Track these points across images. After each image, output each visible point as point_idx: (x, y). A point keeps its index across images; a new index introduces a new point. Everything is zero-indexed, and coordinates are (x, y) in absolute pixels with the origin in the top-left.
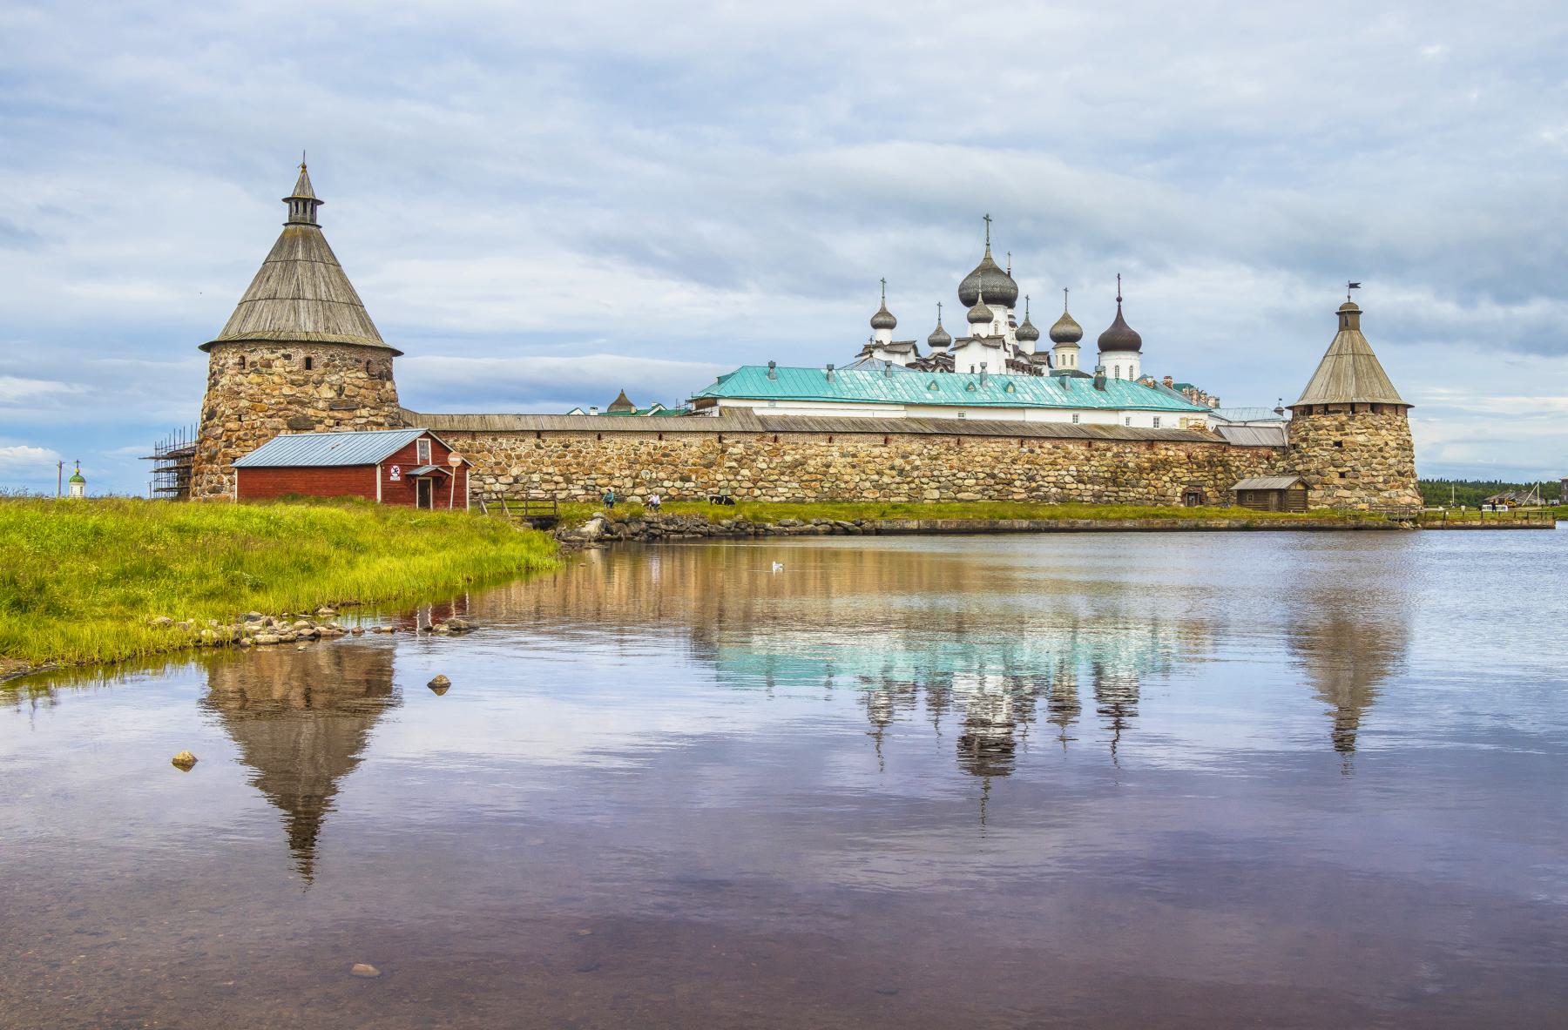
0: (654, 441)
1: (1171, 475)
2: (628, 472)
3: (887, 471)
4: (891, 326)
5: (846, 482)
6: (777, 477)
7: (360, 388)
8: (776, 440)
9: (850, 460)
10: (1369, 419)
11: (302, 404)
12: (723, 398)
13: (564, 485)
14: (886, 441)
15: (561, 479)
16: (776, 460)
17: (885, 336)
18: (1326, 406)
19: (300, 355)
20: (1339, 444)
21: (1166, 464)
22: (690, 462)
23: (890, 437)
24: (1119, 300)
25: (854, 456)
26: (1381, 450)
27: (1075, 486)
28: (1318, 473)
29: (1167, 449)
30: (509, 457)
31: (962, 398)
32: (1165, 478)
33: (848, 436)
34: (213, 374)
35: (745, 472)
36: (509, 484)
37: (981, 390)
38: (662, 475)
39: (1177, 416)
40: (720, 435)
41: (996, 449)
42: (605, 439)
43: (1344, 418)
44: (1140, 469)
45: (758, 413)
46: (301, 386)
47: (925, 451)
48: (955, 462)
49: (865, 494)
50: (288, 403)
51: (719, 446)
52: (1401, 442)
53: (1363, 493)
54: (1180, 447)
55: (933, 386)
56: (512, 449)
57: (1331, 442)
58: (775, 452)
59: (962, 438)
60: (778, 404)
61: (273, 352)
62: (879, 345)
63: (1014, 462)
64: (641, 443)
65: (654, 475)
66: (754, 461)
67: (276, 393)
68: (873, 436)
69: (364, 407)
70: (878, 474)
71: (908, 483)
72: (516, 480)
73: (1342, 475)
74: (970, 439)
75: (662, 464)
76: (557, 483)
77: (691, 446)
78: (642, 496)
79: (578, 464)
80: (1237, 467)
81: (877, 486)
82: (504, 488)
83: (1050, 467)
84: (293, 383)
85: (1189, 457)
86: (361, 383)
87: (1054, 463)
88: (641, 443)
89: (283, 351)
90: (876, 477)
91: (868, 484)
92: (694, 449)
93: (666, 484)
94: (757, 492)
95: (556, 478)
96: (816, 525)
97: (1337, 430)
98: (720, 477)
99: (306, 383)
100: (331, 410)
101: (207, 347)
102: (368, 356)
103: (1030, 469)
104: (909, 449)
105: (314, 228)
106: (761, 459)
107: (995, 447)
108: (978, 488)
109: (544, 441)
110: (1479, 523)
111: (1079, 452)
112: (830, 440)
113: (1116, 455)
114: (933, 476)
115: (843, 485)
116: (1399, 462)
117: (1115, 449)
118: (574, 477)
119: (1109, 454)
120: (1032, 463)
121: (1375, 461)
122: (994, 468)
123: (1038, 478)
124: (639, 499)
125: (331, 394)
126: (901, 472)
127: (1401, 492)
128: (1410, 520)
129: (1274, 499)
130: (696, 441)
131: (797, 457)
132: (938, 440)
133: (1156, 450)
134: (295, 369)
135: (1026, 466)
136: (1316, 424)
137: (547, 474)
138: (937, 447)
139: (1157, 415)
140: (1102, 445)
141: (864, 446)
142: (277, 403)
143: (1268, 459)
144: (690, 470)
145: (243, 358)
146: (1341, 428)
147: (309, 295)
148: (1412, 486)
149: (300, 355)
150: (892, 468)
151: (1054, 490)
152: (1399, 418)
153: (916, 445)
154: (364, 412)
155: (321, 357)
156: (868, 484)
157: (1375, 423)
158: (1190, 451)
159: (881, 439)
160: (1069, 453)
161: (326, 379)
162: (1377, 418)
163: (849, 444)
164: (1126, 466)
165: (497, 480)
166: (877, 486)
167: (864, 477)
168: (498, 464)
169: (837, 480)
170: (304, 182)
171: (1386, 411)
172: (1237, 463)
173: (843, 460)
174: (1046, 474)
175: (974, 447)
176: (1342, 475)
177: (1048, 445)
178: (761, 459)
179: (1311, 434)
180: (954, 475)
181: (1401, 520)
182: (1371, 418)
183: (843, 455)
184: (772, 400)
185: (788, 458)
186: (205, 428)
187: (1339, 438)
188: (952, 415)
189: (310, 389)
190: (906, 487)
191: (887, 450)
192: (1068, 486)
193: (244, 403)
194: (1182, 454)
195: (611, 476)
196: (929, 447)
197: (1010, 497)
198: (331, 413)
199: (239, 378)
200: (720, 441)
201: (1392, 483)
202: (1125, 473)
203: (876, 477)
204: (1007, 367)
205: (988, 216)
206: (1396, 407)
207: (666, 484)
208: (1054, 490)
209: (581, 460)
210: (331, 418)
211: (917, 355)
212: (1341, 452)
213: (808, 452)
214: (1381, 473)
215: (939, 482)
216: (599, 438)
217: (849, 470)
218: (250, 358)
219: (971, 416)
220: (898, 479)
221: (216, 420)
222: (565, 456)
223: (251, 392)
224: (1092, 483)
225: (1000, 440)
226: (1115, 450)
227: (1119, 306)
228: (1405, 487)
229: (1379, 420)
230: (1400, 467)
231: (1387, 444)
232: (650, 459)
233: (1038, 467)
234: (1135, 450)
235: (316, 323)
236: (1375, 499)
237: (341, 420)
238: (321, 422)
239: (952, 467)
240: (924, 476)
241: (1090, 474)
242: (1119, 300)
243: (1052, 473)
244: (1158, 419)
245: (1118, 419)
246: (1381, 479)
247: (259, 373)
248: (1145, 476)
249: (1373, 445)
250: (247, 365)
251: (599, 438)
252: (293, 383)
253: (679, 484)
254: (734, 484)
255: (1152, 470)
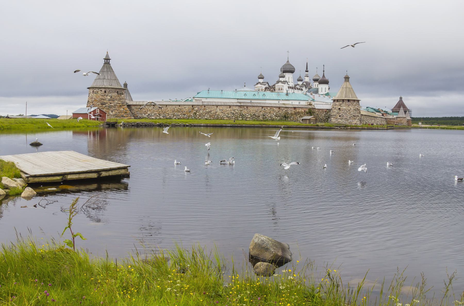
0: (178, 107)
1: (299, 115)
2: (172, 113)
3: (230, 114)
4: (263, 78)
5: (220, 116)
6: (205, 115)
7: (116, 96)
8: (205, 107)
9: (221, 111)
10: (347, 103)
11: (104, 100)
12: (195, 97)
13: (159, 116)
14: (230, 107)
15: (158, 115)
16: (205, 111)
17: (261, 81)
18: (338, 100)
19: (103, 90)
20: (339, 109)
21: (299, 113)
22: (186, 111)
23: (231, 106)
24: (324, 71)
25: (222, 110)
26: (349, 110)
27: (275, 117)
28: (335, 116)
29: (299, 109)
30: (148, 110)
31: (252, 97)
32: (298, 116)
33: (221, 106)
34: (89, 94)
35: (198, 113)
36: (147, 115)
37: (257, 96)
38: (179, 114)
39: (305, 102)
40: (193, 106)
41: (256, 109)
42: (168, 106)
43: (341, 103)
44: (292, 114)
45: (203, 101)
46: (103, 96)
47: (239, 109)
48: (246, 112)
49: (224, 118)
50: (101, 100)
51: (192, 108)
52: (355, 109)
53: (344, 120)
54: (302, 109)
55: (245, 95)
56: (148, 108)
57: (338, 108)
58: (205, 109)
59: (248, 107)
60: (208, 99)
61: (98, 90)
62: (259, 83)
63: (260, 112)
64: (175, 107)
65: (178, 114)
66: (200, 111)
67: (99, 98)
68: (227, 106)
69: (116, 100)
70: (228, 114)
71: (235, 116)
72: (149, 115)
73: (340, 116)
74: (250, 107)
75: (179, 112)
76: (157, 115)
77: (186, 108)
78: (175, 118)
79: (162, 111)
80: (317, 114)
81: (227, 117)
82: (146, 116)
83: (269, 113)
84: (102, 96)
85: (305, 111)
86: (116, 95)
87: (270, 112)
88: (175, 107)
89: (100, 89)
90: (227, 115)
91: (225, 116)
92: (187, 108)
93: (180, 116)
94: (200, 118)
95: (157, 114)
96: (180, 124)
97: (340, 106)
98: (192, 114)
99: (105, 96)
100: (109, 101)
101: (88, 88)
102: (118, 90)
103: (264, 114)
104: (235, 109)
105: (109, 65)
106: (201, 111)
107: (256, 109)
108: (251, 117)
109: (155, 107)
110: (361, 128)
111: (276, 110)
112: (217, 107)
113: (286, 111)
114: (240, 115)
115: (219, 117)
116: (354, 113)
117: (286, 109)
118: (161, 114)
119: (284, 110)
120: (265, 112)
121: (348, 113)
122: (255, 113)
123: (266, 115)
124: (174, 119)
125: (109, 98)
126: (233, 114)
127: (354, 120)
128: (344, 127)
129: (308, 121)
130: (187, 107)
131: (209, 110)
132: (242, 107)
133: (296, 109)
134: (103, 93)
135: (263, 113)
136: (336, 104)
137: (155, 113)
138: (242, 108)
139: (299, 101)
140: (282, 108)
141: (225, 108)
142: (99, 100)
143: (326, 112)
144: (186, 113)
145: (93, 91)
146: (340, 105)
147: (106, 78)
148: (357, 119)
149: (103, 90)
150: (231, 113)
151: (270, 118)
152: (355, 103)
153: (237, 108)
154: (116, 101)
155: (108, 91)
156: (225, 116)
157: (348, 104)
158: (305, 110)
159: (229, 107)
160: (274, 110)
161: (108, 95)
162: (349, 103)
163: (221, 108)
164: (288, 113)
165: (145, 115)
166: (227, 117)
167: (224, 115)
168: (145, 111)
169: (218, 115)
170: (107, 55)
171: (351, 101)
172: (317, 113)
173: (220, 111)
174: (268, 114)
175: (251, 109)
176: (340, 116)
177: (269, 108)
178: (201, 111)
179: (335, 106)
180: (246, 115)
181: (340, 127)
182: (348, 103)
183: (220, 110)
184: (206, 98)
185: (207, 111)
186: (87, 104)
187: (339, 108)
188: (249, 101)
189: (105, 97)
190: (234, 117)
191: (230, 109)
192: (273, 117)
193: (93, 100)
194: (303, 111)
195: (169, 114)
196: (240, 108)
197: (259, 120)
198: (109, 102)
199: (93, 95)
200: (192, 107)
201: (351, 118)
202: (288, 115)
203: (227, 115)
204: (289, 88)
205: (288, 51)
206: (354, 100)
207: (180, 116)
208: (270, 118)
209: (162, 111)
210: (109, 102)
211: (268, 85)
212: (340, 111)
213: (212, 109)
214: (349, 116)
215: (242, 116)
216: (166, 106)
217: (221, 113)
218: (95, 91)
219: (253, 101)
220: (232, 115)
221: (89, 103)
222: (159, 110)
223: (94, 97)
224: (279, 117)
225: (257, 107)
226: (286, 109)
227: (324, 73)
228: (355, 119)
229: (349, 103)
230: (354, 114)
231: (351, 109)
232: (177, 110)
233: (266, 113)
234: (291, 109)
235: (107, 83)
236: (346, 122)
237: (111, 103)
238: (107, 103)
239: (245, 113)
240: (238, 115)
241: (279, 115)
242: (324, 71)
243: (269, 114)
244: (300, 102)
245: (290, 102)
246: (349, 117)
247: (96, 94)
248: (293, 115)
249: (347, 109)
250: (94, 92)
251: (166, 106)
252: (102, 96)
253: (183, 116)
254: (195, 116)
255: (295, 114)
